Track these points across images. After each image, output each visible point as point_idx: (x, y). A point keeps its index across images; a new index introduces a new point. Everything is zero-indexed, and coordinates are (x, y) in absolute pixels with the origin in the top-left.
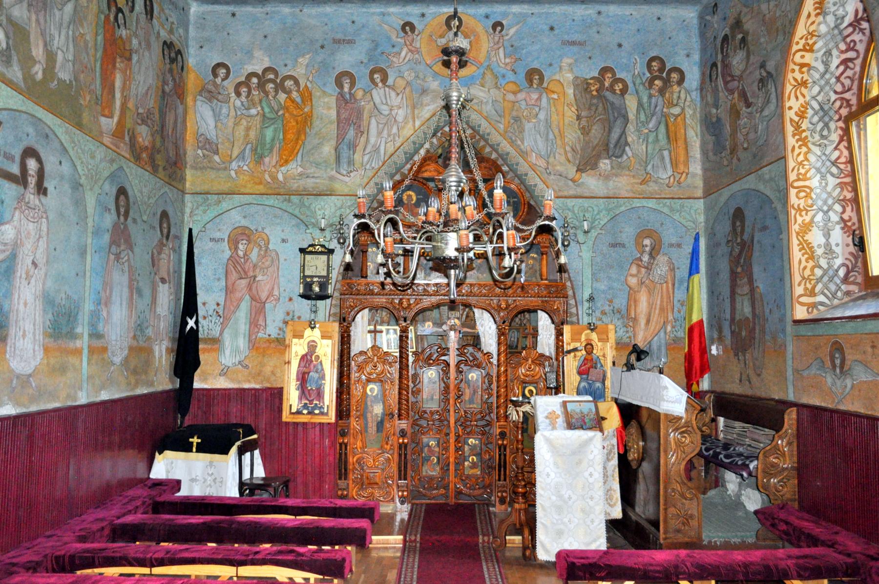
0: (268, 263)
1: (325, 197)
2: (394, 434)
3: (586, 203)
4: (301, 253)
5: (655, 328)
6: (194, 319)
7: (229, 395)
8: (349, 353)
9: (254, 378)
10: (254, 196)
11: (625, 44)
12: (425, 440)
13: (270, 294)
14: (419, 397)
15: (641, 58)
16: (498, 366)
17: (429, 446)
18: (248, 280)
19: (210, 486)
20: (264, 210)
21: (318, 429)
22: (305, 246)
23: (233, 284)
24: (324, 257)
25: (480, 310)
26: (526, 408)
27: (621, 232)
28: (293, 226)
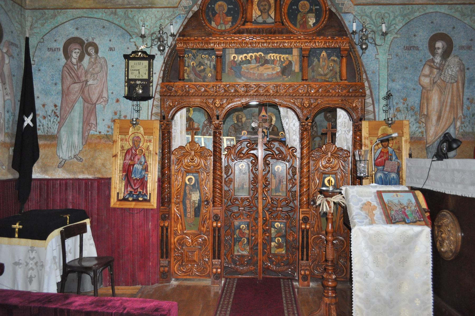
0: (97, 69)
1: (147, 10)
2: (209, 219)
3: (383, 10)
4: (125, 59)
5: (445, 126)
6: (31, 117)
7: (66, 184)
8: (170, 147)
9: (87, 169)
10: (85, 10)
12: (236, 223)
13: (100, 96)
14: (231, 187)
16: (301, 159)
17: (240, 229)
18: (81, 84)
19: (32, 269)
20: (94, 22)
21: (142, 213)
22: (129, 52)
23: (68, 89)
24: (146, 63)
25: (285, 109)
26: (337, 198)
27: (415, 36)
28: (119, 36)
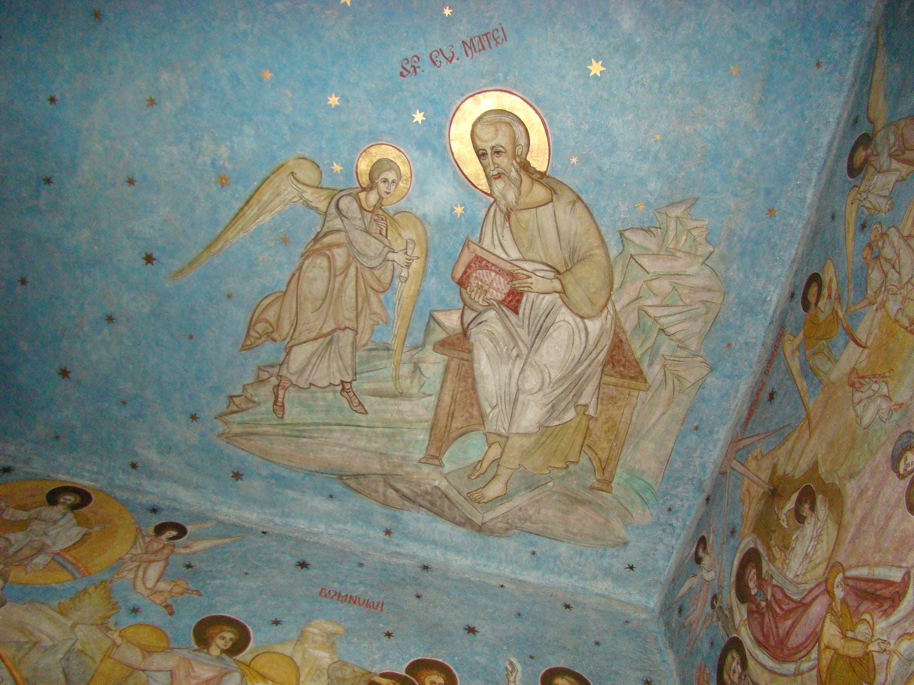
11: (485, 629)
15: (524, 664)
